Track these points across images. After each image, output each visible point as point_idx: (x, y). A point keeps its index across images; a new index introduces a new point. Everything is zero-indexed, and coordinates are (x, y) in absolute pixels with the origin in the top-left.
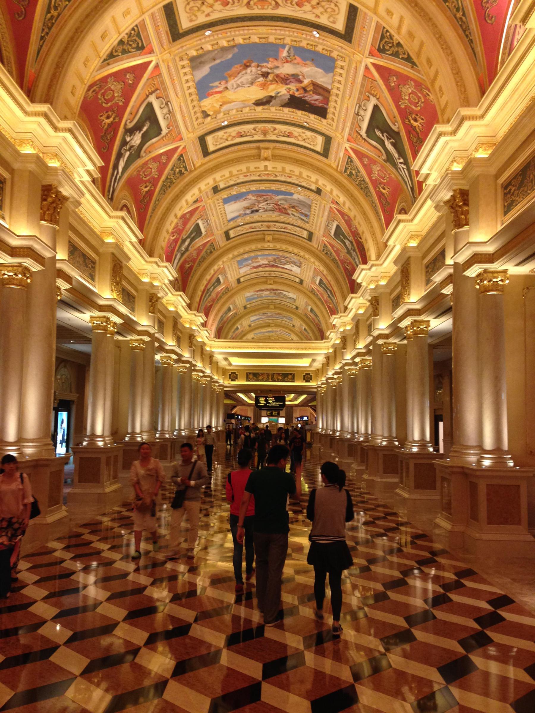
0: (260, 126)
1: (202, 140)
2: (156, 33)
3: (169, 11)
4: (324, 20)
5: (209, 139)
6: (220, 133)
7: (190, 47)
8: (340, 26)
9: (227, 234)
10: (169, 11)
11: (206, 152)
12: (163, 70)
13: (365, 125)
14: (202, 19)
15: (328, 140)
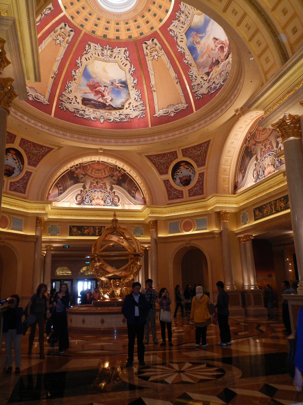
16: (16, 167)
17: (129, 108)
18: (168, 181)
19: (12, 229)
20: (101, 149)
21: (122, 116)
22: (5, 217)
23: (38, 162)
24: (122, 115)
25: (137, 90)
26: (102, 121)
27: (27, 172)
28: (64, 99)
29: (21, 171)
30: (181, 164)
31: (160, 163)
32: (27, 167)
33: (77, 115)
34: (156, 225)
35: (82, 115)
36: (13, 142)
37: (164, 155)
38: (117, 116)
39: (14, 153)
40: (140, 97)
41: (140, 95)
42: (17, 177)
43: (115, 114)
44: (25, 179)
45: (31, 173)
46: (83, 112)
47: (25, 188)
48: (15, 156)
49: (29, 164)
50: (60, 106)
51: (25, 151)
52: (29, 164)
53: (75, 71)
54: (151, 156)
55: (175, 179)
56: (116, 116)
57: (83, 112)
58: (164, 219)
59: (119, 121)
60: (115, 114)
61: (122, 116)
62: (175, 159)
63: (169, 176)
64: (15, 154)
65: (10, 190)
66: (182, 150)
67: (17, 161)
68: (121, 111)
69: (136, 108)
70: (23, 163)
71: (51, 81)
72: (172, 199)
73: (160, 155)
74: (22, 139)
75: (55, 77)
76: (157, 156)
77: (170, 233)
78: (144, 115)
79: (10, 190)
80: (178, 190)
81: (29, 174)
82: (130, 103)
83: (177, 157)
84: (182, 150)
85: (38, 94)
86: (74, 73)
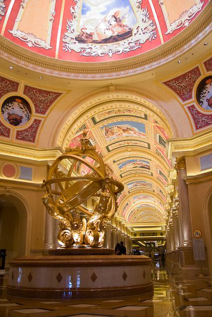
0: (126, 141)
1: (107, 148)
2: (90, 124)
3: (93, 119)
4: (138, 115)
5: (109, 147)
6: (113, 145)
7: (101, 125)
8: (143, 116)
9: (121, 175)
10: (93, 119)
11: (109, 151)
12: (93, 132)
13: (158, 141)
14: (102, 118)
15: (149, 145)
16: (24, 116)
17: (138, 33)
18: (193, 106)
19: (20, 178)
20: (112, 85)
21: (132, 45)
22: (11, 165)
23: (46, 109)
24: (131, 43)
25: (143, 9)
26: (111, 55)
27: (36, 120)
28: (67, 40)
29: (29, 119)
30: (207, 82)
31: (181, 87)
32: (35, 116)
33: (83, 54)
34: (185, 163)
35: (89, 53)
36: (16, 90)
37: (184, 76)
38: (126, 45)
39: (20, 101)
40: (148, 16)
41: (147, 14)
42: (24, 126)
43: (124, 44)
44: (34, 128)
45: (40, 121)
46: (89, 50)
47: (34, 137)
48: (21, 105)
49: (37, 111)
50: (64, 49)
51: (31, 99)
52: (37, 111)
53: (73, 8)
54: (169, 81)
55: (202, 102)
56: (125, 47)
57: (90, 49)
58: (193, 154)
59: (129, 50)
60: (124, 44)
61: (132, 45)
62: (197, 77)
63: (193, 101)
64: (22, 103)
65: (17, 138)
66: (205, 63)
67: (24, 109)
68: (130, 39)
69: (146, 31)
70: (31, 112)
71: (51, 24)
72: (200, 127)
73: (180, 77)
74: (26, 87)
75: (53, 18)
76: (176, 79)
77: (202, 170)
78: (156, 36)
79: (17, 138)
80: (207, 115)
81: (37, 122)
82: (138, 27)
83: (200, 74)
84: (205, 63)
85: (38, 40)
86: (73, 11)
